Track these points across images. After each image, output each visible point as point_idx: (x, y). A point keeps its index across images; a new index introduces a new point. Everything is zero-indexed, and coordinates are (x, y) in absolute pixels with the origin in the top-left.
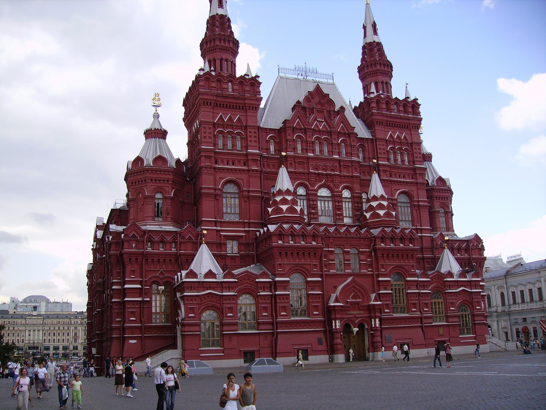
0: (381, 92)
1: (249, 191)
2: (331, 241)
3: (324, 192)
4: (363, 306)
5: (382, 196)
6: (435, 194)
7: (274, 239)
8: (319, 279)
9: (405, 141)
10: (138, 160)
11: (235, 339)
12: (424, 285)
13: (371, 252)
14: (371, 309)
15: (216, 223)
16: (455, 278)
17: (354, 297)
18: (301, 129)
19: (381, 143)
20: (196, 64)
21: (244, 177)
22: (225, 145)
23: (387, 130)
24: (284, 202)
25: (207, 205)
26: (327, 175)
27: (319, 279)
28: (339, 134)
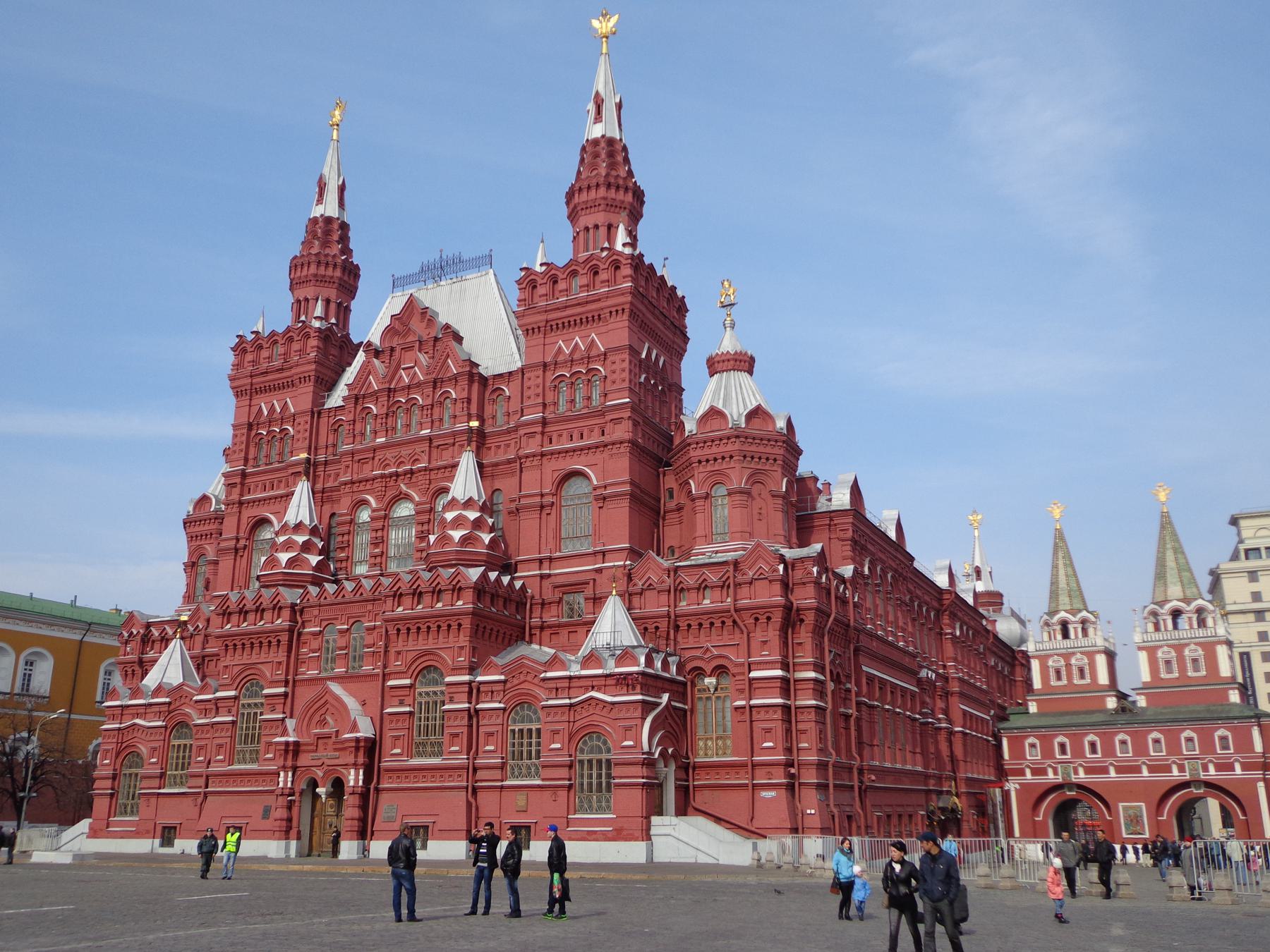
2: (316, 612)
3: (404, 510)
4: (334, 743)
5: (453, 499)
6: (695, 453)
8: (282, 690)
9: (593, 353)
11: (153, 800)
13: (380, 627)
14: (341, 747)
16: (575, 670)
17: (323, 723)
18: (372, 394)
19: (532, 375)
23: (553, 340)
26: (405, 473)
28: (435, 384)
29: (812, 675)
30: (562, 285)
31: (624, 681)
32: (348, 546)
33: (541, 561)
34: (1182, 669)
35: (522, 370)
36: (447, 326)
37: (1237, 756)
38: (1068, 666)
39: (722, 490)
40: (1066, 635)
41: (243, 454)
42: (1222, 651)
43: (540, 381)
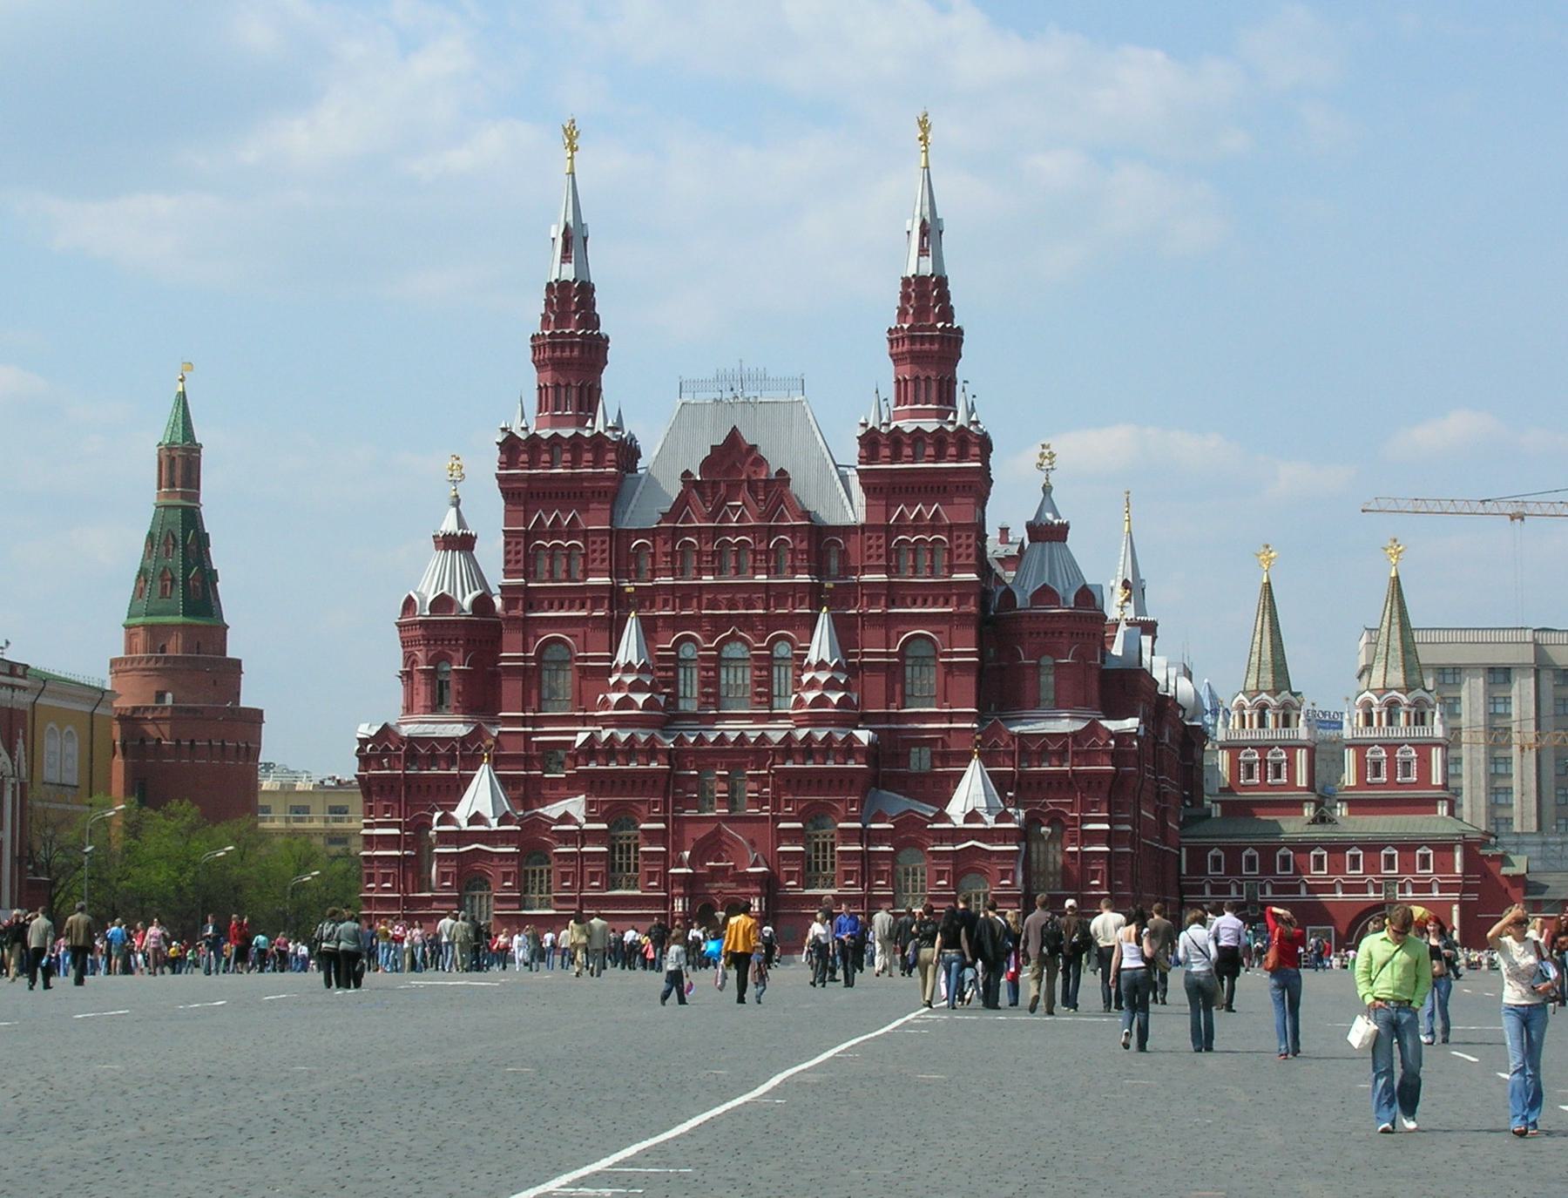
0: (885, 420)
1: (586, 659)
3: (735, 650)
7: (580, 760)
8: (662, 826)
10: (409, 603)
12: (881, 836)
14: (745, 879)
15: (524, 721)
16: (959, 822)
20: (515, 399)
21: (578, 631)
22: (551, 572)
24: (618, 686)
25: (511, 689)
27: (662, 826)
29: (1128, 827)
30: (907, 451)
31: (1004, 836)
32: (674, 683)
33: (888, 717)
34: (1392, 773)
35: (863, 526)
36: (782, 472)
37: (1435, 877)
38: (1263, 762)
39: (1047, 661)
40: (1262, 724)
41: (520, 566)
42: (1436, 755)
43: (882, 541)
